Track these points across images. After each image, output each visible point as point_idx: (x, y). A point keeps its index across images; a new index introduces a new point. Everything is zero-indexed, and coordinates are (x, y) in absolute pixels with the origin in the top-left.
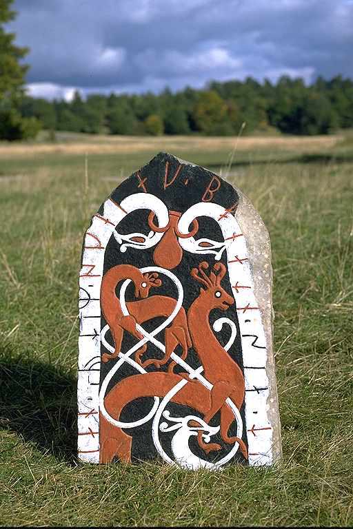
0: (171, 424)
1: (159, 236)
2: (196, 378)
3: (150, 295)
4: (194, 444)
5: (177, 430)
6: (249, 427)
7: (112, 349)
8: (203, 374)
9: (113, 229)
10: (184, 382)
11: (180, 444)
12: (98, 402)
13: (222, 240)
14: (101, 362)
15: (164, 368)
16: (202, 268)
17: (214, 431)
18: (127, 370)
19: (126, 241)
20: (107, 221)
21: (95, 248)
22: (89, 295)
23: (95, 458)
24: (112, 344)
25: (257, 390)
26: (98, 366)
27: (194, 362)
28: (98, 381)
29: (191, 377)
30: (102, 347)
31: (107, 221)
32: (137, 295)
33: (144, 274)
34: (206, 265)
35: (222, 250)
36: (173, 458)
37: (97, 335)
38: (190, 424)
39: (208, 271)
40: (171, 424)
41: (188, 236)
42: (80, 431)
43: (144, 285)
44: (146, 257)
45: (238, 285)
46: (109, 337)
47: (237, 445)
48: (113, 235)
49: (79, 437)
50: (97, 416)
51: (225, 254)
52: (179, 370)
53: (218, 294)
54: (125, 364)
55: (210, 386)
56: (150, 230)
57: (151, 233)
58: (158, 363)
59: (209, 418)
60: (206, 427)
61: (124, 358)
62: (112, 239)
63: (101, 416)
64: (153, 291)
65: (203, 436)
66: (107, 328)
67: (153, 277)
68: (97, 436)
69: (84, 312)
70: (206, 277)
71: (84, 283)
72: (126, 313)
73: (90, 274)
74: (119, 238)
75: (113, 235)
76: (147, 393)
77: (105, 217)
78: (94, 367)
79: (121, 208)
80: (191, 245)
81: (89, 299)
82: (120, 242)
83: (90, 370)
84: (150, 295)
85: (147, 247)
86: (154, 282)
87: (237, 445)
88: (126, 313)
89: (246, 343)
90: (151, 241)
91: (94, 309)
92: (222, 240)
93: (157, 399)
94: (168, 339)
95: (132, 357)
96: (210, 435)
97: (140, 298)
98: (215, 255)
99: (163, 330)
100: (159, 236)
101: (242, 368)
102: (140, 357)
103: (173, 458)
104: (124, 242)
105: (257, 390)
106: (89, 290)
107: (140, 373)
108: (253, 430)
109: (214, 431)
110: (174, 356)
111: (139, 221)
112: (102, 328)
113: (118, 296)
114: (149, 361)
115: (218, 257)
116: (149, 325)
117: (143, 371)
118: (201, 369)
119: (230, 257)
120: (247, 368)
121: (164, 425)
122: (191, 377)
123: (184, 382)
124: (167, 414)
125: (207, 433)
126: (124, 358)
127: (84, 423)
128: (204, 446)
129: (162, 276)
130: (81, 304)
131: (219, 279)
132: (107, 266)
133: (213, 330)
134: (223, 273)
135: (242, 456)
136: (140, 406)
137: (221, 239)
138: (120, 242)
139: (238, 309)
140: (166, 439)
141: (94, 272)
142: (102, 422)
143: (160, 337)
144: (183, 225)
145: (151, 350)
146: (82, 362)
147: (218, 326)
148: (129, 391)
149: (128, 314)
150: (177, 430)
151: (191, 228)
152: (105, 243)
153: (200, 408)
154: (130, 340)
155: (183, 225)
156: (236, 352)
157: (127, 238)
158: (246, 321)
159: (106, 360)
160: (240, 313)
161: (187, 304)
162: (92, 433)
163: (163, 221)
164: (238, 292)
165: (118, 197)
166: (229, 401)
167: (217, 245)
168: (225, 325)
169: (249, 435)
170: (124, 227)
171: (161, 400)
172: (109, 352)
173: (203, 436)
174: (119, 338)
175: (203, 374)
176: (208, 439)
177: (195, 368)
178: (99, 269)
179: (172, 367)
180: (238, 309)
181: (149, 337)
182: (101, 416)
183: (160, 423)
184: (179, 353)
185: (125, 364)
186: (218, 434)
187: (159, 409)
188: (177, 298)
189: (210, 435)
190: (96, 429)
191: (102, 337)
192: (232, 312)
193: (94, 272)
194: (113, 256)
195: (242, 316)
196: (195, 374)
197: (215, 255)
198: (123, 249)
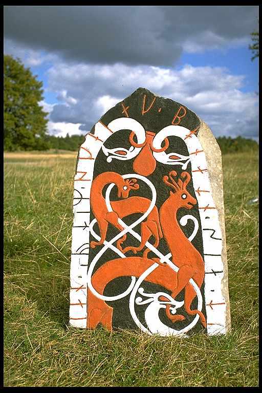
0: (144, 298)
4: (163, 316)
6: (207, 302)
8: (171, 259)
10: (155, 265)
11: (152, 314)
12: (87, 280)
13: (188, 155)
14: (90, 248)
15: (140, 254)
16: (172, 176)
17: (179, 305)
19: (112, 154)
21: (88, 158)
23: (83, 324)
25: (215, 273)
26: (87, 251)
29: (162, 261)
33: (125, 180)
34: (175, 173)
35: (188, 162)
36: (146, 326)
39: (176, 179)
40: (144, 298)
44: (128, 166)
46: (96, 228)
51: (190, 164)
52: (152, 255)
53: (184, 196)
55: (176, 269)
57: (132, 148)
58: (135, 250)
59: (175, 294)
60: (173, 302)
61: (108, 245)
62: (101, 151)
64: (132, 193)
66: (95, 221)
67: (132, 182)
68: (85, 306)
69: (76, 209)
70: (174, 182)
71: (77, 185)
72: (110, 209)
73: (83, 179)
74: (106, 151)
79: (108, 128)
80: (163, 158)
81: (82, 198)
82: (107, 155)
83: (80, 254)
86: (133, 186)
88: (110, 209)
89: (206, 235)
90: (131, 154)
91: (85, 206)
92: (188, 155)
93: (134, 278)
95: (114, 244)
96: (176, 308)
97: (121, 198)
99: (140, 225)
100: (138, 150)
102: (121, 245)
103: (146, 326)
104: (110, 154)
105: (215, 273)
108: (211, 304)
109: (179, 305)
110: (148, 244)
111: (122, 139)
112: (91, 221)
113: (104, 196)
115: (184, 167)
116: (128, 220)
117: (123, 256)
118: (169, 255)
119: (194, 168)
122: (162, 261)
123: (155, 265)
124: (141, 290)
125: (173, 306)
126: (108, 245)
129: (139, 181)
130: (75, 202)
131: (185, 184)
132: (96, 173)
133: (180, 225)
134: (188, 180)
136: (121, 283)
138: (107, 155)
139: (200, 208)
140: (141, 310)
144: (157, 143)
147: (184, 221)
151: (163, 144)
152: (95, 156)
154: (113, 231)
157: (112, 151)
161: (159, 204)
163: (141, 139)
166: (191, 281)
167: (184, 158)
168: (189, 220)
169: (208, 308)
173: (171, 308)
174: (104, 229)
176: (174, 312)
178: (90, 175)
179: (146, 253)
180: (200, 208)
184: (152, 241)
187: (135, 287)
188: (151, 199)
190: (84, 301)
191: (90, 228)
192: (195, 210)
193: (85, 178)
194: (101, 165)
196: (165, 259)
198: (109, 160)
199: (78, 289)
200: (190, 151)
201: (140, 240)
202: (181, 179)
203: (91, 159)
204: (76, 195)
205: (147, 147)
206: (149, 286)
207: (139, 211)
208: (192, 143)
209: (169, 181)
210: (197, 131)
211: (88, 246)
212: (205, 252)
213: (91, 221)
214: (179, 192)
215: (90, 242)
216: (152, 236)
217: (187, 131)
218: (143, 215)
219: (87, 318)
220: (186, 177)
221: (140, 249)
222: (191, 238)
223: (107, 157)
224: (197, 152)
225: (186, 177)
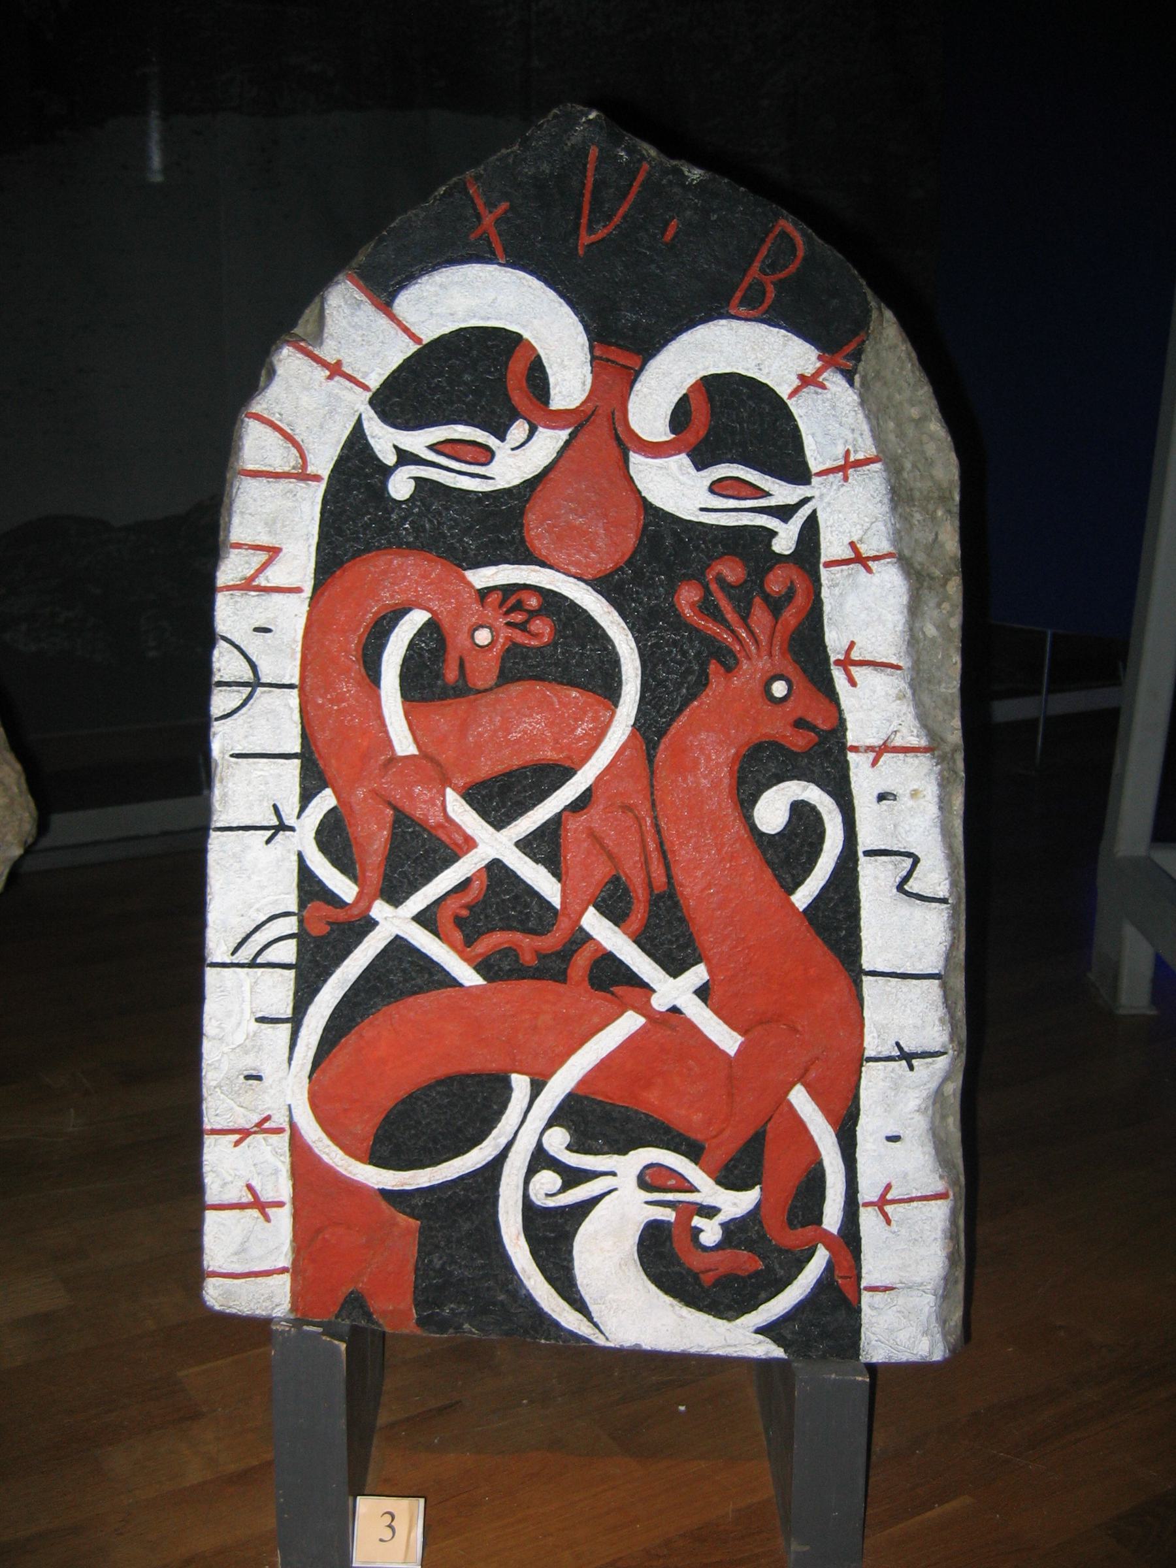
0: (573, 1177)
1: (547, 444)
2: (675, 1010)
3: (506, 677)
5: (594, 1201)
6: (868, 1191)
7: (344, 888)
8: (703, 993)
9: (359, 402)
10: (630, 1023)
11: (605, 1251)
12: (288, 1091)
13: (798, 473)
14: (301, 937)
15: (553, 968)
16: (720, 579)
17: (737, 1203)
18: (402, 969)
20: (335, 370)
22: (253, 667)
23: (272, 1298)
25: (907, 1057)
26: (287, 952)
28: (285, 1009)
29: (659, 1003)
30: (306, 876)
31: (335, 370)
32: (451, 675)
33: (484, 594)
34: (731, 571)
35: (805, 512)
36: (580, 1305)
38: (651, 1179)
40: (573, 1177)
42: (213, 1193)
44: (499, 525)
45: (855, 655)
46: (334, 838)
47: (821, 1258)
48: (359, 422)
49: (210, 1217)
50: (282, 1142)
51: (811, 527)
52: (612, 978)
53: (779, 689)
54: (398, 945)
55: (728, 1040)
56: (514, 415)
57: (519, 430)
58: (528, 945)
60: (708, 1191)
61: (394, 922)
62: (357, 445)
63: (299, 1148)
64: (517, 666)
65: (697, 1221)
66: (326, 800)
67: (518, 607)
68: (283, 1219)
71: (231, 615)
72: (403, 743)
73: (261, 581)
74: (384, 440)
75: (359, 422)
76: (482, 1061)
77: (329, 351)
78: (270, 956)
79: (393, 318)
80: (678, 488)
81: (256, 683)
82: (390, 459)
83: (253, 964)
84: (506, 677)
85: (501, 484)
86: (522, 627)
87: (821, 1258)
88: (403, 743)
89: (874, 880)
90: (521, 456)
91: (276, 722)
92: (798, 473)
93: (520, 1084)
94: (574, 853)
95: (424, 919)
96: (722, 1217)
97: (462, 690)
98: (773, 534)
99: (556, 822)
100: (547, 444)
102: (459, 922)
103: (580, 1305)
104: (405, 458)
105: (907, 1057)
106: (254, 645)
107: (455, 983)
108: (882, 1203)
109: (737, 1203)
110: (594, 923)
111: (471, 378)
115: (785, 539)
116: (499, 799)
117: (468, 976)
118: (698, 974)
119: (832, 546)
121: (547, 1180)
122: (659, 1003)
123: (630, 1023)
124: (557, 1141)
125: (709, 1212)
126: (394, 922)
127: (224, 1167)
128: (696, 1262)
129: (553, 602)
130: (221, 701)
132: (331, 560)
133: (753, 828)
134: (800, 600)
137: (795, 470)
138: (390, 459)
139: (855, 749)
140: (553, 1233)
141: (275, 576)
143: (544, 846)
144: (650, 406)
147: (772, 812)
148: (408, 1051)
149: (412, 750)
150: (594, 1201)
151: (680, 417)
152: (323, 462)
153: (688, 1117)
154: (417, 851)
155: (650, 406)
156: (839, 913)
157: (418, 441)
158: (882, 797)
159: (319, 929)
160: (859, 769)
161: (650, 727)
162: (260, 1205)
163: (570, 379)
164: (853, 683)
166: (800, 1099)
167: (783, 493)
168: (801, 812)
169: (868, 1219)
170: (403, 398)
172: (332, 899)
173: (697, 1221)
174: (374, 837)
175: (703, 993)
176: (711, 1233)
177: (675, 969)
178: (298, 564)
179: (582, 961)
180: (855, 749)
181: (495, 845)
182: (299, 1148)
183: (531, 1171)
184: (615, 913)
185: (398, 945)
186: (754, 1215)
187: (526, 1121)
188: (611, 692)
190: (281, 1188)
191: (304, 835)
193: (275, 576)
195: (864, 778)
196: (675, 991)
197: (773, 534)
198: (400, 486)
199: (245, 1133)
200: (816, 457)
201: (556, 902)
203: (303, 475)
204: (225, 663)
205: (601, 428)
206: (598, 1120)
207: (548, 754)
208: (831, 420)
210: (857, 356)
211: (290, 925)
213: (306, 798)
214: (752, 668)
215: (302, 904)
216: (615, 880)
218: (565, 773)
219: (296, 1270)
220: (790, 595)
221: (551, 941)
222: (803, 897)
224: (846, 467)
225: (790, 595)
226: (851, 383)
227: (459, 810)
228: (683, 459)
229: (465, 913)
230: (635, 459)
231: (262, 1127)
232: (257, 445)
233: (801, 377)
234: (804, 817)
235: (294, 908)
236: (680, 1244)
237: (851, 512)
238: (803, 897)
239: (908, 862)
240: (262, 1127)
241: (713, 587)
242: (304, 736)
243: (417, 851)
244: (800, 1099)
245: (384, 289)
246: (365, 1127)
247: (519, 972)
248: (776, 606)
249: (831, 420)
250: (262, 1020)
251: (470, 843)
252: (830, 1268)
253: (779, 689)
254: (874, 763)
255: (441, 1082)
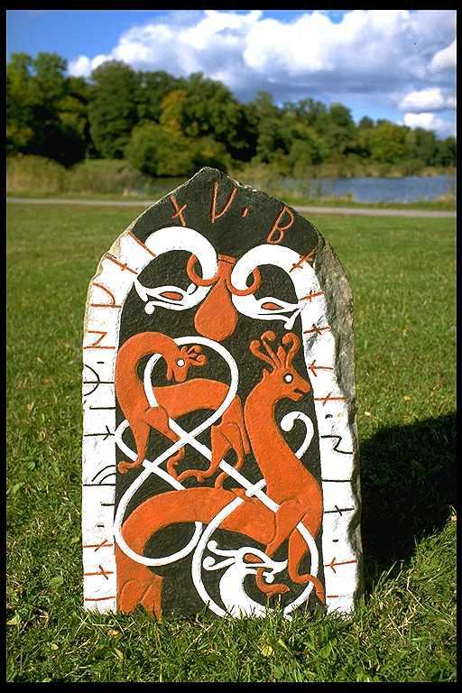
0: (219, 559)
4: (250, 585)
5: (228, 567)
6: (327, 561)
8: (264, 490)
10: (239, 501)
12: (113, 530)
13: (294, 300)
14: (117, 473)
15: (209, 482)
16: (266, 339)
17: (279, 567)
18: (155, 485)
19: (155, 297)
20: (124, 267)
21: (108, 306)
23: (109, 606)
24: (133, 448)
25: (340, 511)
26: (112, 480)
27: (253, 475)
28: (111, 500)
29: (248, 494)
31: (124, 267)
32: (169, 376)
35: (296, 314)
36: (223, 607)
37: (109, 434)
40: (219, 559)
41: (242, 294)
43: (181, 363)
44: (182, 322)
46: (128, 437)
47: (311, 586)
51: (299, 317)
52: (230, 483)
53: (289, 378)
55: (273, 506)
56: (190, 282)
58: (199, 475)
59: (272, 547)
60: (269, 563)
61: (151, 467)
62: (133, 296)
63: (118, 550)
64: (192, 372)
65: (265, 574)
66: (125, 424)
68: (113, 578)
69: (89, 401)
71: (89, 357)
72: (153, 402)
74: (143, 292)
78: (105, 482)
79: (145, 247)
80: (250, 307)
81: (99, 382)
82: (145, 299)
83: (100, 484)
84: (188, 378)
85: (186, 307)
87: (311, 586)
88: (153, 402)
89: (325, 446)
90: (192, 298)
91: (106, 396)
92: (294, 300)
93: (199, 525)
95: (163, 466)
96: (274, 572)
97: (173, 382)
101: (320, 481)
102: (174, 467)
103: (223, 607)
104: (151, 298)
105: (340, 511)
106: (97, 368)
107: (174, 489)
108: (332, 565)
109: (279, 567)
110: (224, 466)
111: (172, 268)
112: (117, 425)
113: (142, 378)
114: (186, 473)
116: (188, 422)
117: (178, 486)
118: (262, 483)
119: (306, 326)
120: (327, 481)
121: (209, 561)
122: (248, 494)
123: (239, 501)
124: (213, 546)
125: (270, 570)
126: (151, 467)
127: (90, 560)
128: (263, 588)
129: (205, 349)
130: (86, 389)
131: (292, 354)
132: (125, 334)
133: (280, 428)
135: (317, 601)
136: (176, 535)
138: (145, 299)
139: (316, 399)
140: (212, 580)
141: (103, 343)
142: (121, 557)
143: (204, 438)
144: (239, 278)
145: (190, 458)
146: (88, 473)
147: (287, 423)
148: (157, 514)
149: (157, 405)
150: (228, 567)
151: (250, 281)
152: (121, 299)
154: (158, 442)
155: (239, 278)
156: (312, 461)
157: (155, 292)
158: (327, 417)
160: (318, 404)
161: (243, 393)
162: (103, 573)
165: (142, 235)
166: (301, 527)
167: (288, 307)
168: (298, 422)
169: (327, 571)
171: (205, 526)
173: (265, 574)
174: (142, 438)
175: (264, 490)
176: (270, 578)
178: (113, 339)
180: (316, 399)
181: (187, 438)
182: (118, 550)
183: (203, 558)
184: (232, 462)
187: (200, 540)
188: (229, 383)
189: (274, 572)
190: (112, 566)
192: (306, 403)
193: (103, 343)
194: (133, 317)
196: (253, 489)
198: (149, 309)
200: (299, 294)
202: (283, 346)
203: (113, 305)
204: (87, 375)
205: (222, 286)
207: (207, 406)
208: (304, 279)
209: (262, 349)
211: (113, 470)
212: (324, 476)
213: (117, 425)
214: (279, 370)
217: (294, 257)
218: (214, 411)
222: (299, 454)
223: (144, 304)
225: (292, 343)
226: (312, 266)
227: (173, 425)
228: (252, 297)
229: (177, 463)
230: (234, 297)
231: (104, 544)
232: (95, 295)
233: (294, 265)
234: (299, 424)
235: (115, 464)
236: (259, 583)
237: (313, 313)
238: (299, 454)
239: (338, 439)
240: (104, 544)
241: (265, 343)
242: (116, 401)
243: (158, 442)
244: (301, 527)
245: (142, 235)
246: (141, 542)
247: (196, 484)
248: (287, 348)
249: (304, 279)
250: (104, 505)
251: (177, 438)
252: (314, 589)
253: (289, 378)
254: (324, 403)
255: (172, 525)
